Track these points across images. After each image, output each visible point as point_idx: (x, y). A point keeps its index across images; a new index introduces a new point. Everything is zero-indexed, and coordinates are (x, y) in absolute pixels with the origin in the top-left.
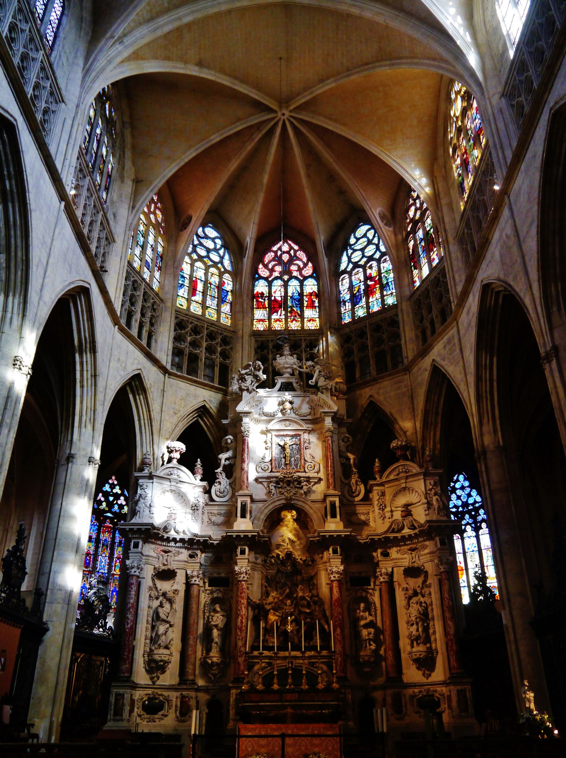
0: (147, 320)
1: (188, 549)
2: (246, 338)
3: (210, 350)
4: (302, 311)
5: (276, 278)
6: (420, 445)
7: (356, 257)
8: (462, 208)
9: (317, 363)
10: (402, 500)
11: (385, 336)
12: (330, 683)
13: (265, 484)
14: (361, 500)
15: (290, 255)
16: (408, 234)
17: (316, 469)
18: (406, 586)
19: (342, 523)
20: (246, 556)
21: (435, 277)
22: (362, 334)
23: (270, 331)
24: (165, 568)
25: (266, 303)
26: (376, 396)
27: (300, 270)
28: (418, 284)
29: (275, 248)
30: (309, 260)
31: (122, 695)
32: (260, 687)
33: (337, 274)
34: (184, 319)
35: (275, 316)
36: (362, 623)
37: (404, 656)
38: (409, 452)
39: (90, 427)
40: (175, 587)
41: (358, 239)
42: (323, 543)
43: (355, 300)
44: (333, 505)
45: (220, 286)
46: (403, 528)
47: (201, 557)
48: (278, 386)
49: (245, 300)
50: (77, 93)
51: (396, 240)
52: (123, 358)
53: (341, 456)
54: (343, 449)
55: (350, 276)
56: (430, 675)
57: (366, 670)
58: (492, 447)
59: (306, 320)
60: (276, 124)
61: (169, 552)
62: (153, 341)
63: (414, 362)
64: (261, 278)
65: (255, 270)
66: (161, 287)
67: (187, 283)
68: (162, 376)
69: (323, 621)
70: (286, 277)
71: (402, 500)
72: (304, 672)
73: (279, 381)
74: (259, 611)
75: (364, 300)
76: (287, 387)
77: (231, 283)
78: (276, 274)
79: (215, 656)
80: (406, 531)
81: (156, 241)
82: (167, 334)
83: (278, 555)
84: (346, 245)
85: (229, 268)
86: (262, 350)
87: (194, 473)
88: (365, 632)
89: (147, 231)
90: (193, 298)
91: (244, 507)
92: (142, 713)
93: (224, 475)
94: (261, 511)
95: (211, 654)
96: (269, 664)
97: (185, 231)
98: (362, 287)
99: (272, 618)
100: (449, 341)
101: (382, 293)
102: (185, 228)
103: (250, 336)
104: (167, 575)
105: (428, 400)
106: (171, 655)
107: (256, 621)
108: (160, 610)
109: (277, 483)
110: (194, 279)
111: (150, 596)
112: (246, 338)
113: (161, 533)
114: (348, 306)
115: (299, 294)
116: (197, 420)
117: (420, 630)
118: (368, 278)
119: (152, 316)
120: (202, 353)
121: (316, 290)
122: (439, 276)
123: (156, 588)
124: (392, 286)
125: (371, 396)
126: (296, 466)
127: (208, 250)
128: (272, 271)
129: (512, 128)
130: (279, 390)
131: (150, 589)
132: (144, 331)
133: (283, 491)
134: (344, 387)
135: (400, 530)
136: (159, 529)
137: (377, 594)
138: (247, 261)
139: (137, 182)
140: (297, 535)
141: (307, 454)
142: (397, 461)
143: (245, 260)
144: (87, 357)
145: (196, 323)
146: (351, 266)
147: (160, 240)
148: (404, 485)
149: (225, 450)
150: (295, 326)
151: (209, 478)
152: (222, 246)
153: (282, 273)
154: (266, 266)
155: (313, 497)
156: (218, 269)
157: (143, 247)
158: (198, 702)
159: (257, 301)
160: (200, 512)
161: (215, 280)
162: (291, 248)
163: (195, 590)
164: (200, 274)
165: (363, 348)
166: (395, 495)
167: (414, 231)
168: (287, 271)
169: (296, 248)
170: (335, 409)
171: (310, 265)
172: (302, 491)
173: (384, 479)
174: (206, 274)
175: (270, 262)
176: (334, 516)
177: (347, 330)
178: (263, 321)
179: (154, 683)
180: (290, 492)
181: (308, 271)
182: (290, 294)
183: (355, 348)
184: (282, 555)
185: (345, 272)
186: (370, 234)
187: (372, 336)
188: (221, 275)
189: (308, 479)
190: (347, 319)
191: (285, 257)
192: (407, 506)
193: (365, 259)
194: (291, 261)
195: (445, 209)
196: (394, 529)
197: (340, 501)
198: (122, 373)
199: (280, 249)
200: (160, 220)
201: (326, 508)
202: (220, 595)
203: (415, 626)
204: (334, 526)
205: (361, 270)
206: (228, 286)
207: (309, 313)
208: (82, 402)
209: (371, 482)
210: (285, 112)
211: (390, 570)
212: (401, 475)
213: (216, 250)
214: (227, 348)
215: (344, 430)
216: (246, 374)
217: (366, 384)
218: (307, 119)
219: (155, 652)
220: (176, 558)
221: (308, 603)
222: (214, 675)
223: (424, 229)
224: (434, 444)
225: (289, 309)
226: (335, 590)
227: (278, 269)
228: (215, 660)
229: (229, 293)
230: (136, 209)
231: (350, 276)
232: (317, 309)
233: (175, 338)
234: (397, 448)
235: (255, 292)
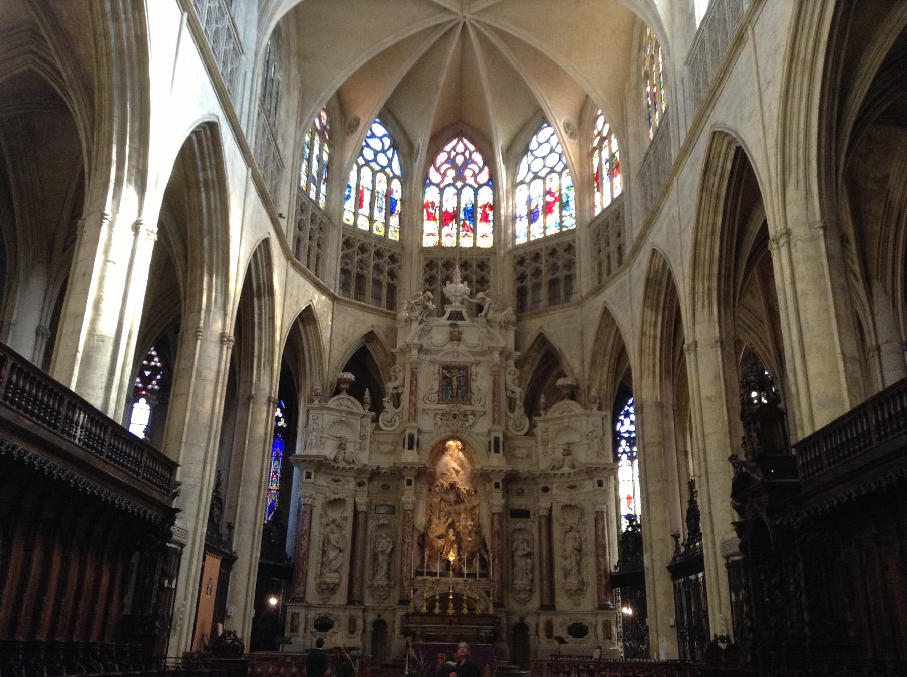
0: (315, 244)
1: (356, 477)
2: (415, 256)
3: (377, 268)
4: (475, 225)
5: (449, 185)
6: (586, 383)
7: (537, 166)
8: (651, 136)
9: (488, 295)
10: (564, 438)
11: (560, 263)
12: (488, 609)
13: (432, 416)
14: (526, 434)
15: (465, 157)
16: (594, 149)
17: (482, 403)
18: (562, 521)
19: (504, 460)
20: (412, 487)
21: (616, 210)
22: (537, 257)
23: (440, 247)
24: (337, 497)
25: (438, 212)
26: (546, 328)
27: (475, 175)
28: (597, 211)
29: (448, 148)
30: (485, 164)
31: (298, 614)
32: (424, 610)
34: (352, 236)
35: (446, 230)
36: (520, 552)
37: (558, 586)
38: (573, 394)
39: (268, 368)
40: (346, 514)
41: (540, 144)
43: (532, 216)
44: (497, 440)
45: (388, 195)
46: (563, 467)
48: (447, 315)
50: (255, 38)
51: (581, 155)
52: (295, 293)
53: (506, 389)
54: (510, 383)
55: (529, 188)
56: (580, 605)
57: (522, 596)
58: (649, 401)
59: (478, 236)
60: (457, 24)
61: (339, 480)
62: (320, 263)
63: (586, 297)
64: (432, 184)
65: (426, 176)
67: (353, 194)
68: (330, 303)
69: (483, 551)
70: (459, 184)
71: (564, 438)
72: (465, 598)
73: (449, 310)
75: (541, 216)
77: (400, 191)
78: (449, 180)
79: (381, 580)
80: (566, 470)
81: (321, 149)
82: (334, 256)
83: (442, 485)
85: (398, 172)
86: (431, 270)
87: (363, 403)
88: (522, 563)
89: (312, 139)
90: (360, 211)
92: (314, 630)
93: (391, 403)
94: (427, 442)
95: (378, 577)
96: (432, 588)
97: (353, 136)
98: (541, 203)
100: (621, 286)
101: (561, 212)
102: (353, 132)
103: (419, 253)
104: (336, 503)
105: (597, 339)
106: (340, 578)
108: (331, 536)
109: (443, 414)
110: (361, 188)
111: (322, 524)
112: (415, 256)
113: (332, 464)
114: (525, 221)
115: (473, 205)
116: (365, 347)
117: (574, 563)
118: (549, 193)
119: (320, 237)
120: (370, 274)
121: (491, 202)
122: (617, 210)
123: (327, 515)
124: (572, 204)
125: (541, 328)
126: (463, 398)
128: (444, 175)
129: (690, 104)
130: (449, 319)
131: (322, 516)
132: (312, 255)
133: (449, 423)
134: (514, 318)
135: (559, 469)
136: (330, 460)
137: (536, 526)
140: (461, 465)
141: (474, 386)
142: (562, 399)
143: (416, 165)
144: (265, 300)
145: (363, 240)
146: (531, 176)
147: (326, 148)
148: (567, 424)
149: (393, 378)
150: (466, 242)
152: (390, 146)
153: (456, 179)
154: (438, 170)
156: (386, 174)
157: (309, 160)
158: (364, 621)
159: (428, 211)
160: (368, 441)
161: (382, 188)
162: (466, 148)
163: (361, 517)
164: (366, 182)
165: (537, 273)
166: (558, 432)
167: (600, 147)
168: (460, 176)
169: (472, 147)
170: (503, 344)
171: (486, 169)
172: (467, 424)
173: (548, 416)
174: (373, 182)
175: (443, 164)
176: (497, 451)
177: (522, 252)
178: (433, 235)
179: (325, 603)
180: (456, 424)
181: (484, 177)
182: (462, 206)
184: (446, 485)
185: (522, 183)
186: (554, 140)
187: (547, 261)
189: (473, 413)
191: (460, 160)
192: (568, 444)
193: (547, 170)
195: (631, 138)
196: (554, 467)
197: (505, 437)
198: (295, 308)
199: (454, 148)
200: (324, 122)
201: (490, 443)
202: (386, 522)
203: (569, 560)
204: (497, 462)
205: (541, 181)
206: (397, 196)
208: (260, 344)
209: (536, 418)
210: (465, 14)
211: (549, 505)
212: (565, 414)
213: (384, 151)
214: (396, 266)
215: (512, 362)
216: (417, 304)
217: (537, 314)
218: (488, 22)
219: (327, 575)
220: (346, 487)
221: (470, 532)
222: (380, 597)
223: (610, 149)
224: (601, 384)
225: (462, 223)
226: (496, 522)
227: (452, 173)
228: (380, 583)
229: (398, 203)
230: (304, 124)
231: (529, 188)
232: (492, 223)
233: (342, 258)
234: (564, 387)
235: (425, 202)
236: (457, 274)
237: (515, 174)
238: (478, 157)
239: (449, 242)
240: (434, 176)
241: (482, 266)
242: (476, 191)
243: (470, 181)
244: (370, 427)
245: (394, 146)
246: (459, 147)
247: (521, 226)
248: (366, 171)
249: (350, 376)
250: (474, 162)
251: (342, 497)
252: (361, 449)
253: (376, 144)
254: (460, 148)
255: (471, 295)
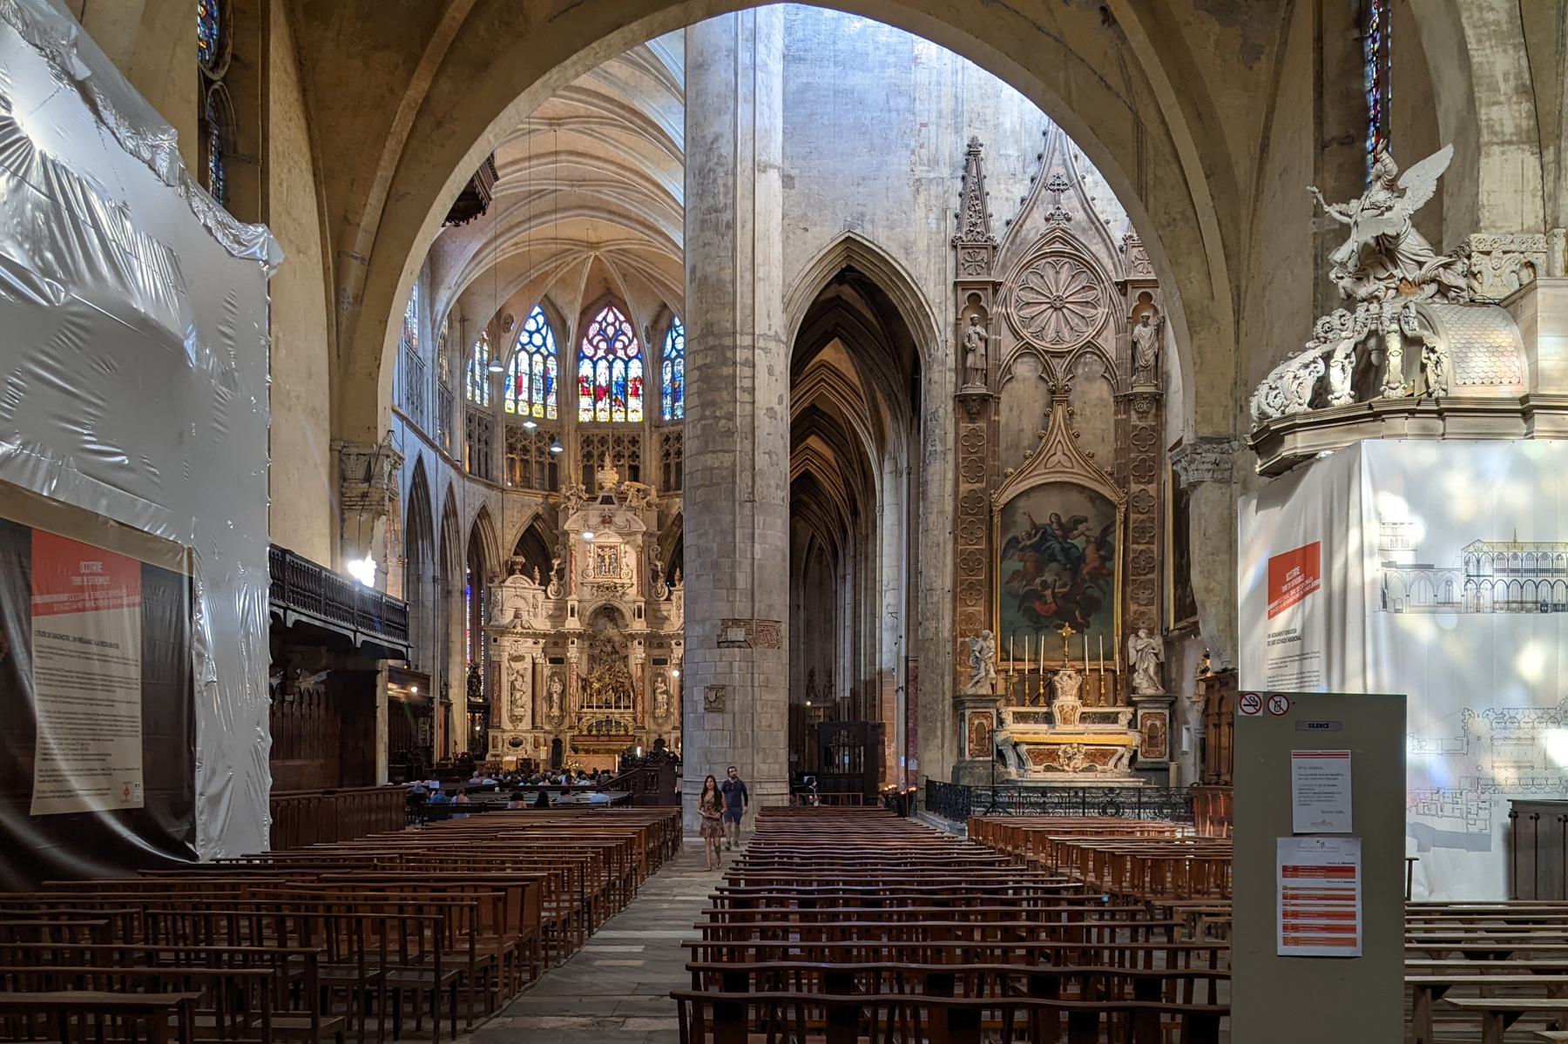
2: (572, 433)
27: (625, 348)
29: (599, 318)
33: (660, 359)
35: (600, 405)
42: (633, 637)
44: (640, 609)
45: (545, 376)
47: (542, 641)
49: (570, 387)
64: (585, 357)
66: (490, 400)
70: (611, 357)
74: (585, 684)
76: (607, 500)
78: (601, 353)
84: (671, 327)
85: (552, 348)
87: (533, 579)
88: (660, 698)
91: (572, 609)
99: (596, 685)
107: (584, 689)
127: (531, 334)
128: (596, 348)
138: (571, 344)
139: (463, 320)
146: (674, 354)
150: (619, 417)
151: (545, 582)
154: (590, 342)
155: (626, 598)
157: (473, 371)
161: (538, 369)
162: (616, 318)
164: (524, 367)
169: (622, 318)
174: (530, 365)
181: (632, 351)
183: (672, 451)
188: (545, 359)
190: (667, 417)
191: (611, 331)
194: (616, 337)
199: (605, 319)
204: (639, 626)
206: (553, 374)
207: (634, 403)
213: (538, 331)
227: (603, 345)
236: (608, 460)
237: (662, 349)
238: (626, 327)
239: (603, 417)
240: (588, 350)
241: (634, 442)
242: (626, 363)
243: (621, 353)
244: (541, 596)
245: (547, 323)
246: (609, 316)
247: (667, 401)
248: (523, 356)
249: (521, 559)
250: (624, 334)
251: (521, 652)
252: (535, 616)
253: (531, 325)
254: (611, 319)
255: (620, 483)
